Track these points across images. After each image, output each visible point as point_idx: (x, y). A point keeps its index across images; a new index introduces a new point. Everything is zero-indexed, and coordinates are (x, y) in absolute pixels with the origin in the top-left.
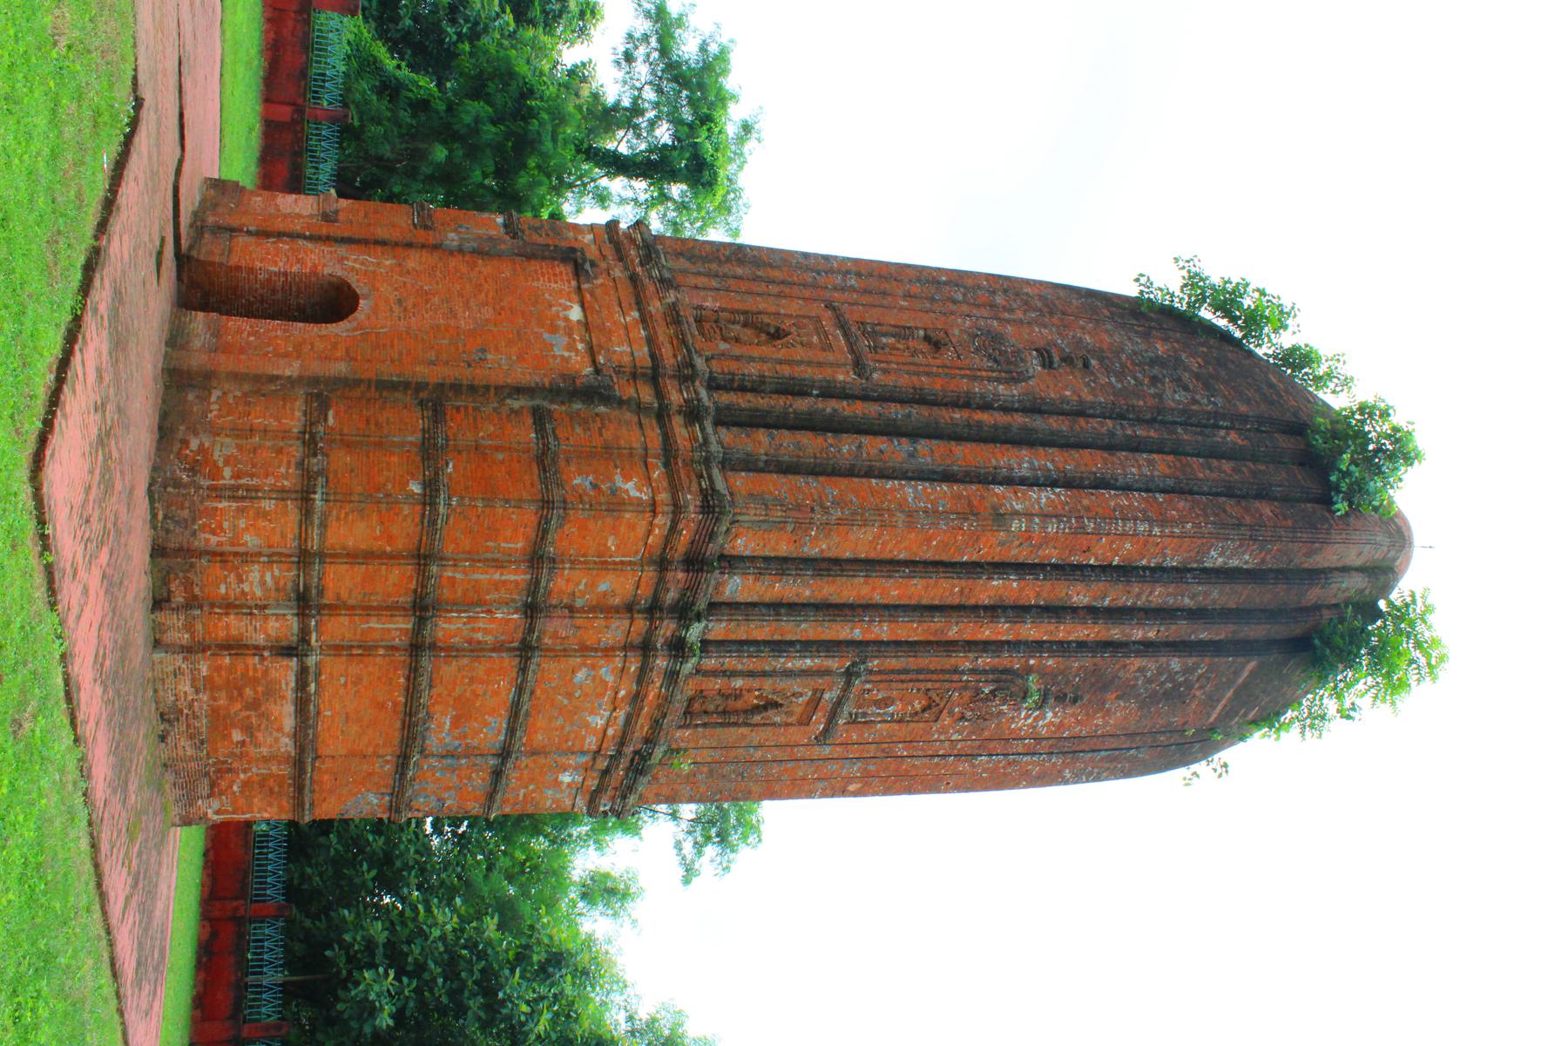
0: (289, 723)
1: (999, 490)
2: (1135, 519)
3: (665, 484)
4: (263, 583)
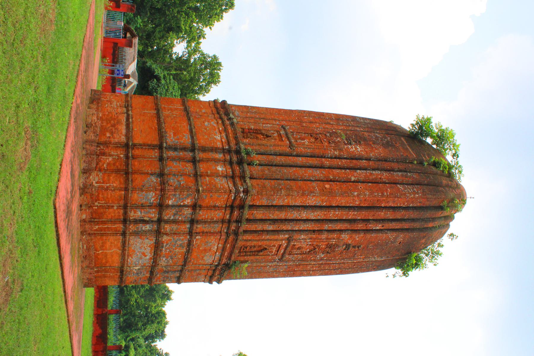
0: (124, 132)
4: (117, 105)
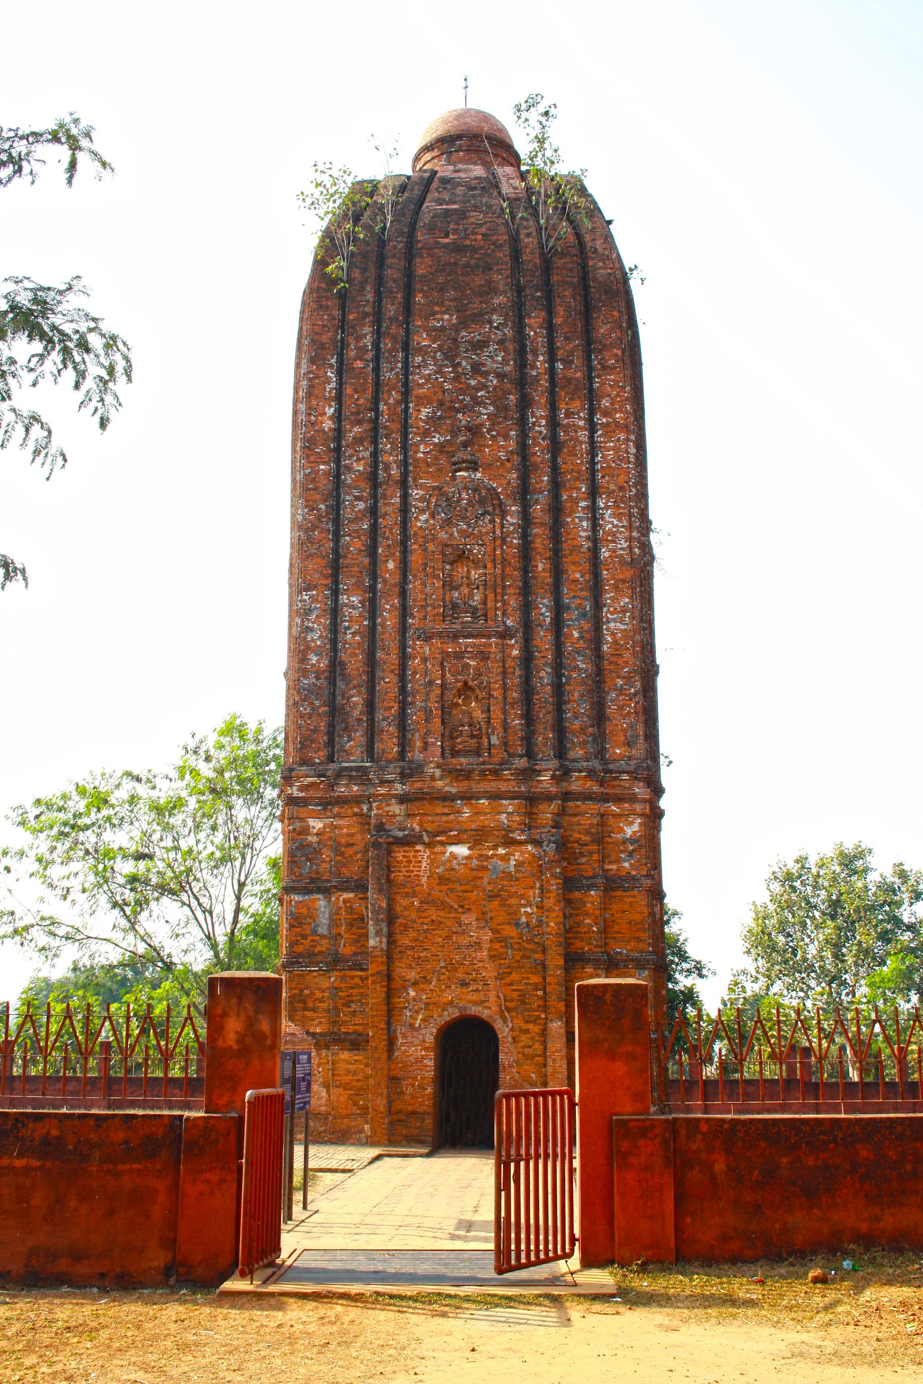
1: (605, 553)
2: (628, 453)
3: (626, 805)
